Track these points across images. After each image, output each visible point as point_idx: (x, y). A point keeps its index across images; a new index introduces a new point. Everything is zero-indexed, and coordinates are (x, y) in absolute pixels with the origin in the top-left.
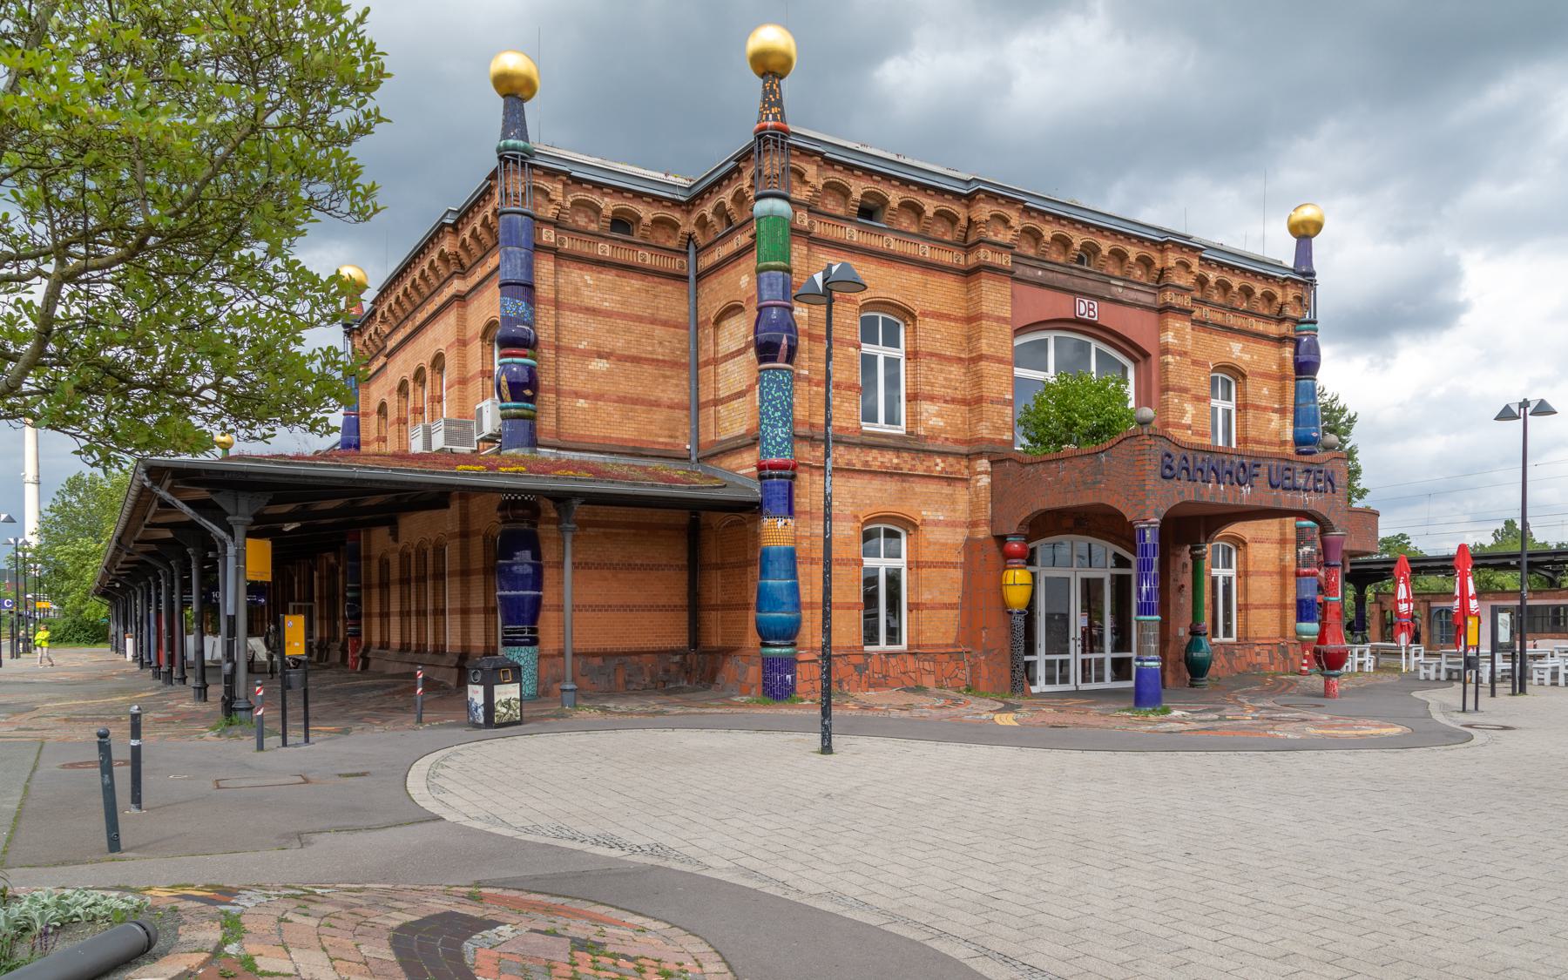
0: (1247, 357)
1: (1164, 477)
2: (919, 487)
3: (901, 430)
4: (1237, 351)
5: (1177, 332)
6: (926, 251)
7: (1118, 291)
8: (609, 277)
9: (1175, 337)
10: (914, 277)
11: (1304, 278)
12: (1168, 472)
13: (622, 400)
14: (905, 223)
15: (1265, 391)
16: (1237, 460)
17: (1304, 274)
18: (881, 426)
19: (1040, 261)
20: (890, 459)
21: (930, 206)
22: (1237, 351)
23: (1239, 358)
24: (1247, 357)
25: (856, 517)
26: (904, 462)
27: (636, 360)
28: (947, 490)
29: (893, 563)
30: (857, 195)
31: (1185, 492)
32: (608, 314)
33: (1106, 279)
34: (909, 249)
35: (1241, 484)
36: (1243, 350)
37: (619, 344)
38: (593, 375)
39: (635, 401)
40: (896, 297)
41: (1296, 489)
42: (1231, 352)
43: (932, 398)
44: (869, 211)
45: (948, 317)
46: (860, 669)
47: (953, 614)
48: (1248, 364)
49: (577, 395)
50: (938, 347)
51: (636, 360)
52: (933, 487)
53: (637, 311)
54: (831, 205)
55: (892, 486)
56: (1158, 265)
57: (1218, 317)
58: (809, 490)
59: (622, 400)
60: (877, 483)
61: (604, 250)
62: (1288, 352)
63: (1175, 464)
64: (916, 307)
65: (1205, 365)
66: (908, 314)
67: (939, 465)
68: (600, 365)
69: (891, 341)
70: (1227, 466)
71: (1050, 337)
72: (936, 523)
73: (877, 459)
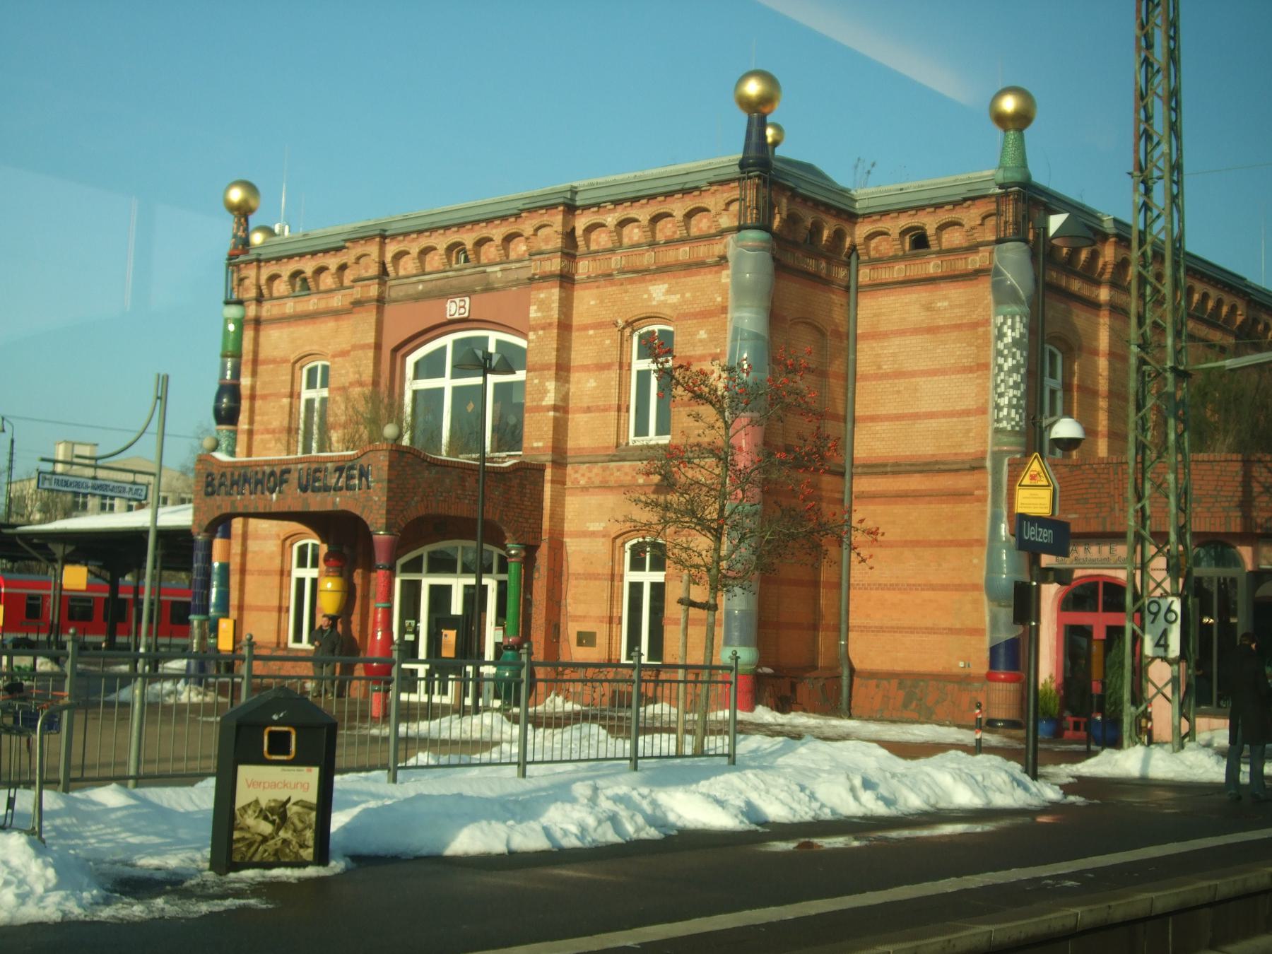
0: (674, 299)
1: (207, 494)
5: (542, 305)
9: (539, 310)
10: (329, 325)
12: (210, 489)
15: (703, 334)
22: (658, 293)
23: (664, 304)
24: (674, 299)
25: (278, 536)
35: (272, 491)
36: (669, 292)
41: (326, 489)
42: (650, 295)
48: (674, 307)
63: (216, 483)
65: (615, 324)
70: (260, 476)
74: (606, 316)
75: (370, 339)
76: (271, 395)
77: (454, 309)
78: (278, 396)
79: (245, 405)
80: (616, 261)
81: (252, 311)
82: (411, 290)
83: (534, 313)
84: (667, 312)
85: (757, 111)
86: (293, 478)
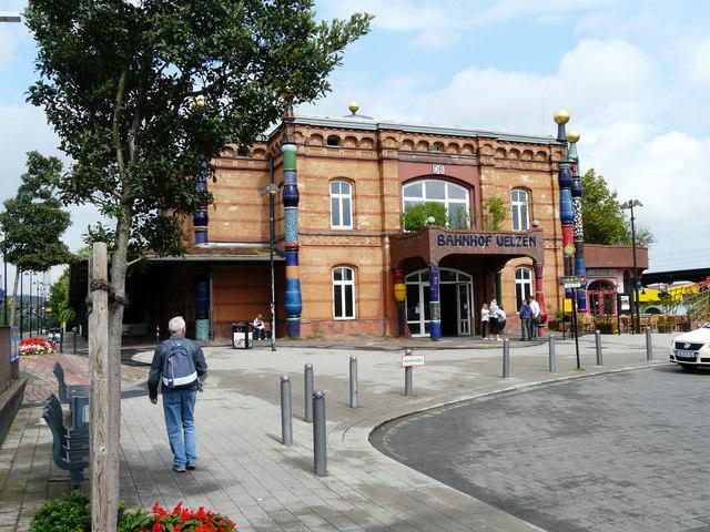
0: (532, 182)
2: (357, 251)
3: (350, 228)
4: (525, 179)
6: (359, 154)
7: (456, 159)
8: (237, 173)
10: (354, 165)
11: (564, 142)
13: (242, 221)
14: (350, 144)
16: (478, 236)
17: (562, 141)
18: (341, 227)
19: (414, 152)
20: (344, 240)
21: (359, 136)
22: (525, 179)
24: (532, 182)
26: (351, 241)
27: (248, 205)
28: (371, 251)
29: (349, 283)
30: (326, 137)
31: (450, 250)
32: (236, 188)
33: (449, 156)
34: (352, 154)
37: (241, 199)
38: (231, 213)
39: (249, 221)
40: (346, 175)
43: (363, 214)
44: (334, 141)
45: (370, 180)
46: (331, 327)
47: (374, 303)
49: (224, 221)
50: (366, 193)
51: (248, 205)
52: (364, 250)
53: (249, 185)
54: (316, 142)
55: (345, 251)
56: (475, 147)
57: (514, 165)
58: (304, 255)
59: (242, 221)
60: (339, 250)
61: (235, 164)
62: (556, 177)
64: (355, 177)
65: (507, 187)
66: (351, 180)
67: (367, 241)
68: (235, 208)
69: (345, 191)
71: (423, 183)
72: (367, 266)
73: (337, 241)
74: (504, 182)
75: (396, 176)
76: (316, 194)
77: (437, 170)
78: (321, 195)
79: (301, 197)
80: (507, 163)
81: (302, 150)
82: (409, 157)
83: (483, 178)
84: (528, 186)
85: (562, 122)
86: (494, 239)
